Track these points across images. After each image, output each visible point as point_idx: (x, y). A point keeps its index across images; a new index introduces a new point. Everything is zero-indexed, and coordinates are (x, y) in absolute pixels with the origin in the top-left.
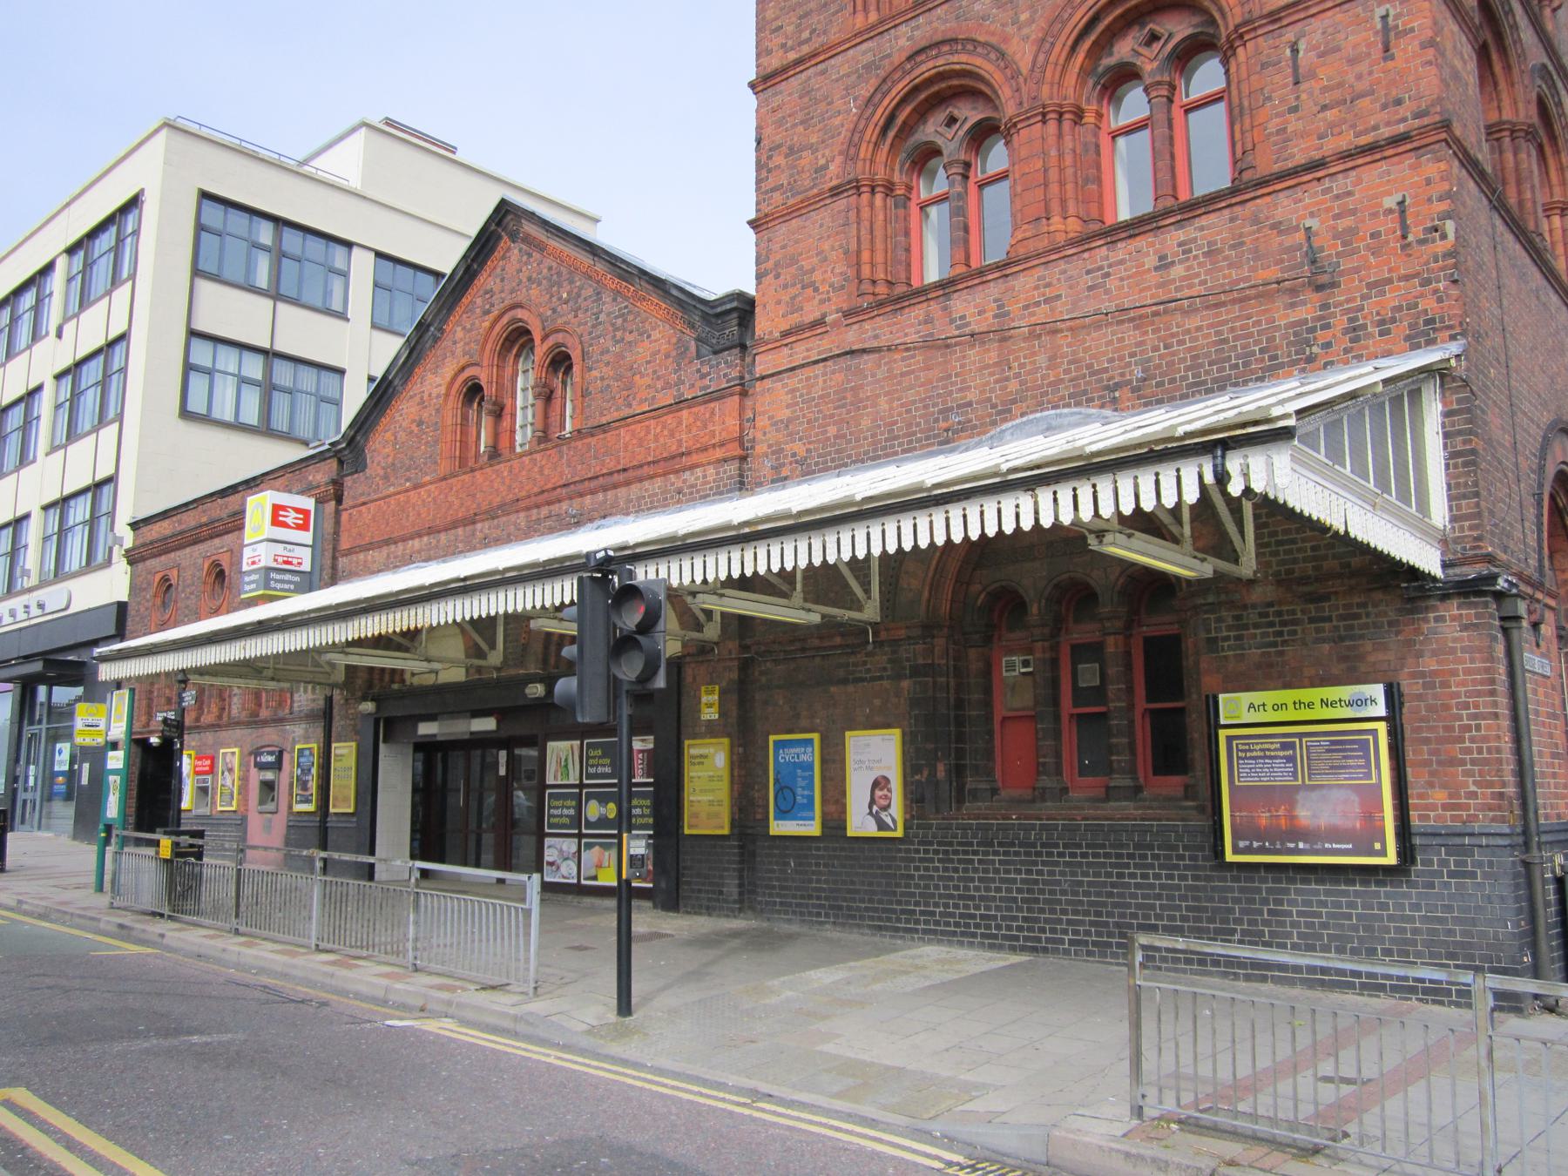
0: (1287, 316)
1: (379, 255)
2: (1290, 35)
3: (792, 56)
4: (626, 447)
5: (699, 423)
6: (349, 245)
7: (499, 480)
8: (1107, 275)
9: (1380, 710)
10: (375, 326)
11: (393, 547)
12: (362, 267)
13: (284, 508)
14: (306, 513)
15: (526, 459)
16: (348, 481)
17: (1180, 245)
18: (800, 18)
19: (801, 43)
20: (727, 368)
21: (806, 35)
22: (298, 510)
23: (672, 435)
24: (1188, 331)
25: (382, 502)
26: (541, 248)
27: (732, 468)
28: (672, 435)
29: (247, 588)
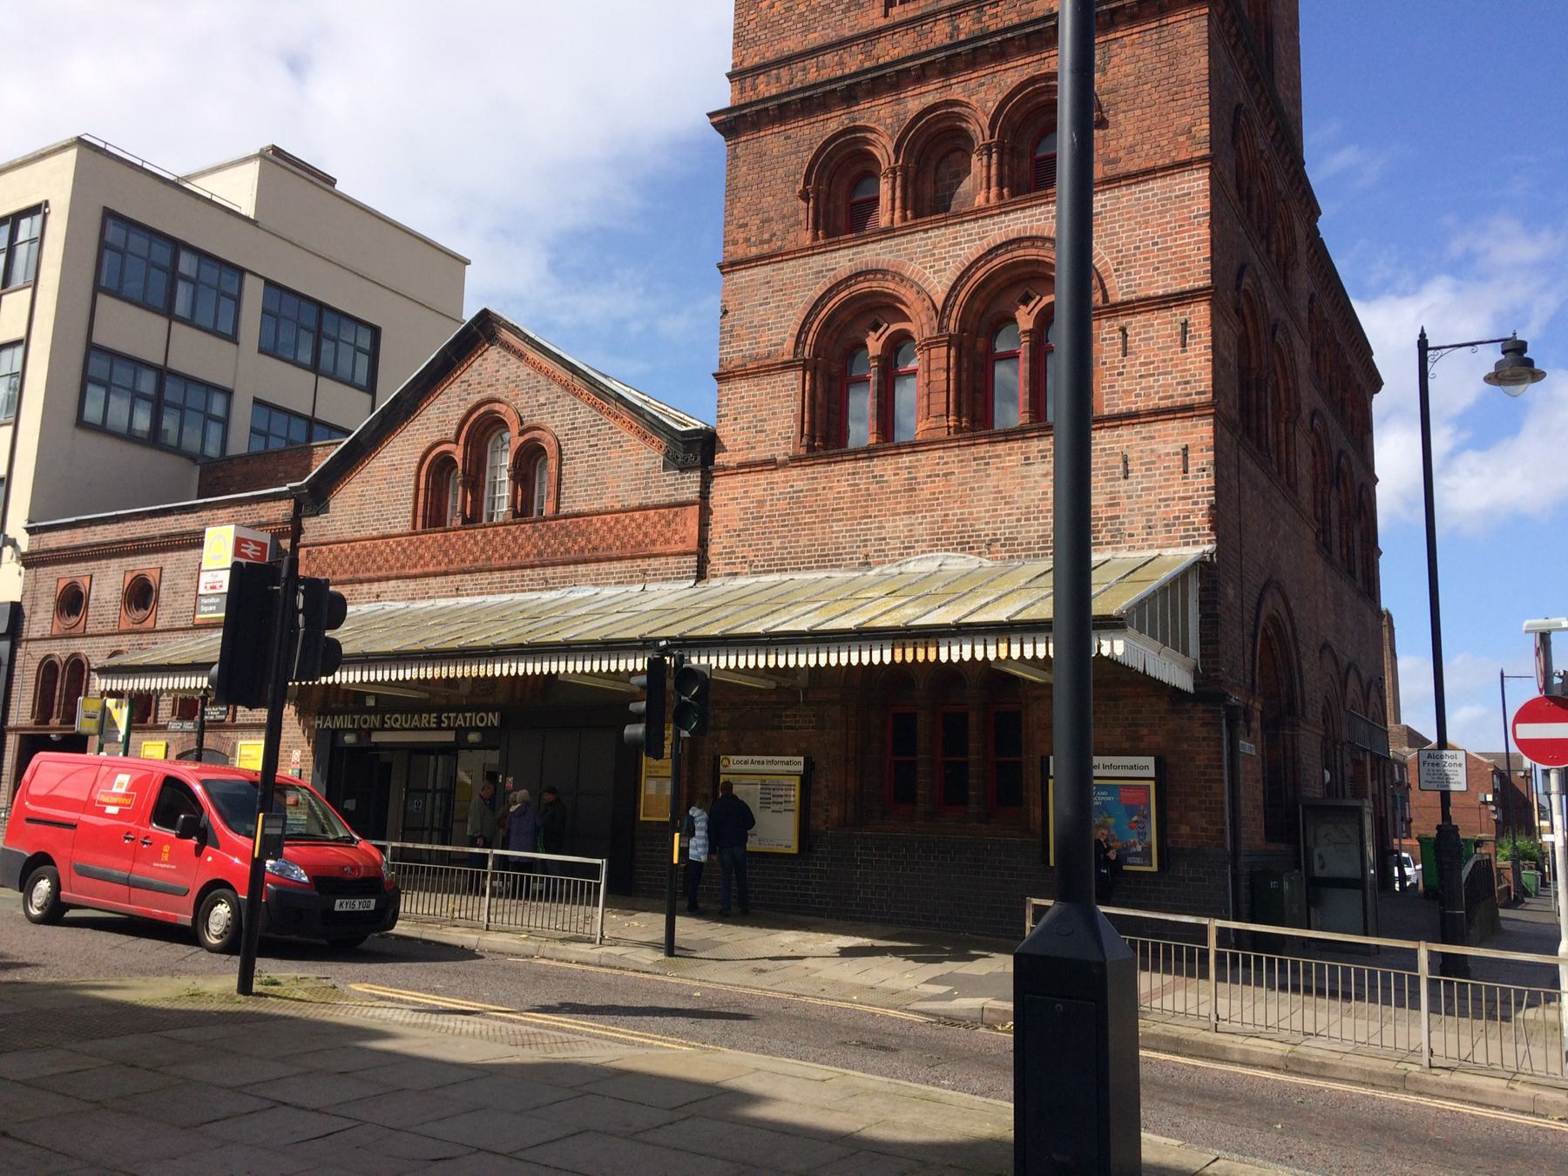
0: (1107, 512)
1: (269, 283)
2: (1123, 321)
3: (754, 251)
4: (597, 531)
5: (663, 522)
6: (241, 271)
7: (472, 541)
8: (988, 464)
9: (1151, 773)
10: (261, 351)
11: (358, 586)
12: (253, 293)
13: (245, 541)
14: (263, 545)
15: (501, 529)
16: (307, 523)
17: (1039, 451)
18: (763, 222)
19: (762, 242)
20: (689, 486)
21: (766, 236)
22: (255, 543)
23: (639, 527)
24: (1041, 512)
25: (346, 545)
26: (521, 356)
27: (692, 561)
28: (639, 527)
29: (203, 609)
